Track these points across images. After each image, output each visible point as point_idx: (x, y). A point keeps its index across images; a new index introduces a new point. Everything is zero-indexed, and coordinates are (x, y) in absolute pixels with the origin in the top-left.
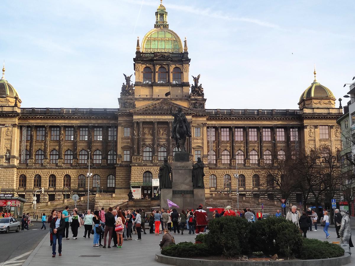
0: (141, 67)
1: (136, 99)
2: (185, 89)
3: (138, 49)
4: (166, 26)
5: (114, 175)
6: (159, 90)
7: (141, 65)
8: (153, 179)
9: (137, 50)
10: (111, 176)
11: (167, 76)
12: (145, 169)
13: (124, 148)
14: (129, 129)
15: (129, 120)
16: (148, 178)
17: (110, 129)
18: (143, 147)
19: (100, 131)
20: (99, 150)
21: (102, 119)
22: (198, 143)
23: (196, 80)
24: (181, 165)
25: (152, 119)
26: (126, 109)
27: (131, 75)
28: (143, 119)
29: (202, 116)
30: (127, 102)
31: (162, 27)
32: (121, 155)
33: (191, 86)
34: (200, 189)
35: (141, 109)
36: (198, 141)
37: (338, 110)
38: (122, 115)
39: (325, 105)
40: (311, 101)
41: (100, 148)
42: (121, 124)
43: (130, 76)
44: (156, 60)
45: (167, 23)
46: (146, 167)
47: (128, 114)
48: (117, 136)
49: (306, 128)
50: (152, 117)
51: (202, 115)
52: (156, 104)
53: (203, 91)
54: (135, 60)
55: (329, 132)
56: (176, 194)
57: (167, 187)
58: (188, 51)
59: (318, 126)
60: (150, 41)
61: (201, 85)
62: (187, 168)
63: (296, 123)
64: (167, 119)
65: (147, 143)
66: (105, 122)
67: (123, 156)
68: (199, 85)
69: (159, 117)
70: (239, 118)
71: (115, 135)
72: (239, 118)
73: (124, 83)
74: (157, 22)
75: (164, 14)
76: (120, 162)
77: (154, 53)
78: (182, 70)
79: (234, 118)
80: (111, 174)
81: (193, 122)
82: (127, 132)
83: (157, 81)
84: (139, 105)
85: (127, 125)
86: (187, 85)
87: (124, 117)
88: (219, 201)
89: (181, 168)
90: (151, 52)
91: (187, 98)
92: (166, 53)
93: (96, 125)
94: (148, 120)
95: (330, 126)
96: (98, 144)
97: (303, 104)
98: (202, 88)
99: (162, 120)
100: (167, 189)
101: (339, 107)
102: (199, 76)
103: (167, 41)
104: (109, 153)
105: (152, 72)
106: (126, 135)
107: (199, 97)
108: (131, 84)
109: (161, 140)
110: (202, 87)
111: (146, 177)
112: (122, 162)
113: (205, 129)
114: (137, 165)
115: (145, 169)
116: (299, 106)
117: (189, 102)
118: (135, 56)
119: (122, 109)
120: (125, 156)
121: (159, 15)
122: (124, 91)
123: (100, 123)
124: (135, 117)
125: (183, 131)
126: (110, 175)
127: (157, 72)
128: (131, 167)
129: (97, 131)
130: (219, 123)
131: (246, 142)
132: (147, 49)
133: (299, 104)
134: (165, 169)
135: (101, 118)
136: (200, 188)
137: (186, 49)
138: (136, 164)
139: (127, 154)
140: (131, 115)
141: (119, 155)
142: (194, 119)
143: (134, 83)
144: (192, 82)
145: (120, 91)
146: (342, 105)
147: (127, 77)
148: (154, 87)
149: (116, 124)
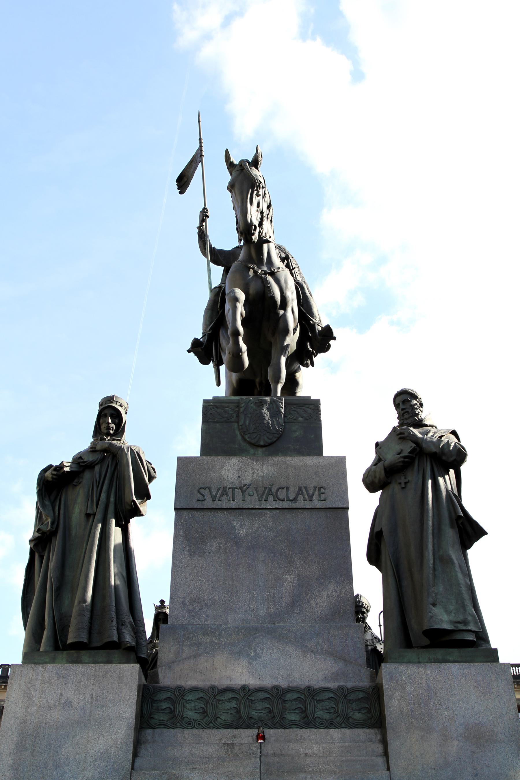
24: (248, 479)
34: (455, 668)
56: (190, 724)
62: (301, 503)
89: (252, 502)
100: (78, 661)
136: (455, 652)
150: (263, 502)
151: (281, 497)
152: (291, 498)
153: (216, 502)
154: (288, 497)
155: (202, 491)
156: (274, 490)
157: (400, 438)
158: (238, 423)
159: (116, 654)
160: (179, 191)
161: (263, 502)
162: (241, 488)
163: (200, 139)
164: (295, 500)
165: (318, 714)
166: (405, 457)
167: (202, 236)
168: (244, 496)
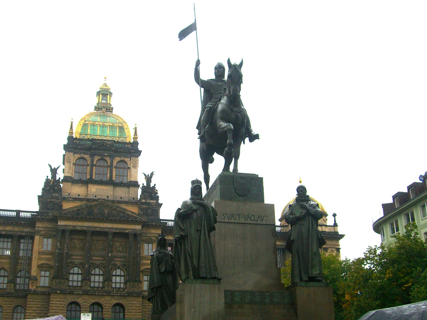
0: (73, 157)
1: (64, 199)
2: (132, 189)
3: (71, 133)
4: (109, 109)
5: (24, 307)
6: (96, 188)
7: (74, 155)
8: (82, 314)
9: (70, 135)
10: (19, 308)
11: (109, 172)
12: (70, 299)
13: (41, 267)
14: (50, 241)
15: (52, 228)
16: (73, 313)
17: (22, 241)
18: (69, 266)
19: (8, 242)
20: (5, 270)
21: (12, 224)
23: (149, 179)
25: (85, 227)
26: (48, 212)
27: (59, 167)
28: (72, 226)
29: (156, 227)
30: (51, 202)
31: (104, 110)
32: (36, 277)
33: (141, 186)
35: (70, 212)
37: (333, 228)
38: (42, 220)
41: (6, 267)
42: (38, 232)
43: (58, 168)
44: (95, 149)
45: (112, 106)
46: (71, 296)
47: (50, 219)
48: (32, 250)
50: (86, 224)
51: (156, 225)
52: (91, 206)
53: (157, 193)
54: (66, 147)
57: (204, 275)
58: (138, 141)
60: (87, 125)
61: (155, 185)
62: (259, 222)
64: (107, 228)
65: (77, 262)
66: (16, 229)
67: (39, 279)
68: (152, 185)
69: (96, 225)
71: (29, 248)
73: (47, 177)
74: (98, 104)
75: (107, 95)
76: (34, 288)
77: (93, 140)
78: (129, 165)
80: (19, 305)
81: (143, 235)
82: (47, 244)
83: (94, 178)
84: (66, 206)
85: (48, 235)
86: (136, 184)
87: (46, 223)
89: (242, 220)
90: (88, 139)
91: (134, 202)
92: (108, 140)
93: (4, 233)
94: (78, 228)
96: (4, 261)
98: (157, 190)
99: (99, 229)
101: (334, 224)
102: (152, 174)
103: (110, 127)
104: (19, 275)
105: (88, 165)
106: (45, 249)
107: (152, 202)
108: (57, 179)
109: (94, 258)
110: (156, 189)
111: (71, 311)
112: (37, 287)
114: (59, 292)
115: (70, 299)
117: (139, 207)
118: (66, 142)
119: (42, 211)
120: (42, 278)
121: (101, 95)
122: (47, 187)
123: (9, 231)
124: (61, 223)
125: (239, 115)
126: (17, 306)
127: (95, 165)
128: (49, 294)
129: (4, 241)
132: (83, 134)
134: (195, 215)
135: (12, 223)
137: (135, 138)
138: (58, 290)
139: (45, 276)
140: (55, 220)
141: (34, 276)
142: (144, 230)
143: (62, 178)
144: (142, 181)
145: (42, 186)
147: (53, 168)
148: (89, 185)
149: (32, 232)
150: (246, 221)
151: (253, 219)
152: (256, 219)
153: (229, 220)
154: (254, 219)
155: (224, 215)
156: (250, 216)
157: (301, 207)
158: (233, 185)
159: (216, 281)
160: (179, 39)
161: (246, 221)
162: (238, 215)
163: (195, 20)
164: (257, 221)
165: (275, 300)
166: (303, 215)
168: (239, 218)
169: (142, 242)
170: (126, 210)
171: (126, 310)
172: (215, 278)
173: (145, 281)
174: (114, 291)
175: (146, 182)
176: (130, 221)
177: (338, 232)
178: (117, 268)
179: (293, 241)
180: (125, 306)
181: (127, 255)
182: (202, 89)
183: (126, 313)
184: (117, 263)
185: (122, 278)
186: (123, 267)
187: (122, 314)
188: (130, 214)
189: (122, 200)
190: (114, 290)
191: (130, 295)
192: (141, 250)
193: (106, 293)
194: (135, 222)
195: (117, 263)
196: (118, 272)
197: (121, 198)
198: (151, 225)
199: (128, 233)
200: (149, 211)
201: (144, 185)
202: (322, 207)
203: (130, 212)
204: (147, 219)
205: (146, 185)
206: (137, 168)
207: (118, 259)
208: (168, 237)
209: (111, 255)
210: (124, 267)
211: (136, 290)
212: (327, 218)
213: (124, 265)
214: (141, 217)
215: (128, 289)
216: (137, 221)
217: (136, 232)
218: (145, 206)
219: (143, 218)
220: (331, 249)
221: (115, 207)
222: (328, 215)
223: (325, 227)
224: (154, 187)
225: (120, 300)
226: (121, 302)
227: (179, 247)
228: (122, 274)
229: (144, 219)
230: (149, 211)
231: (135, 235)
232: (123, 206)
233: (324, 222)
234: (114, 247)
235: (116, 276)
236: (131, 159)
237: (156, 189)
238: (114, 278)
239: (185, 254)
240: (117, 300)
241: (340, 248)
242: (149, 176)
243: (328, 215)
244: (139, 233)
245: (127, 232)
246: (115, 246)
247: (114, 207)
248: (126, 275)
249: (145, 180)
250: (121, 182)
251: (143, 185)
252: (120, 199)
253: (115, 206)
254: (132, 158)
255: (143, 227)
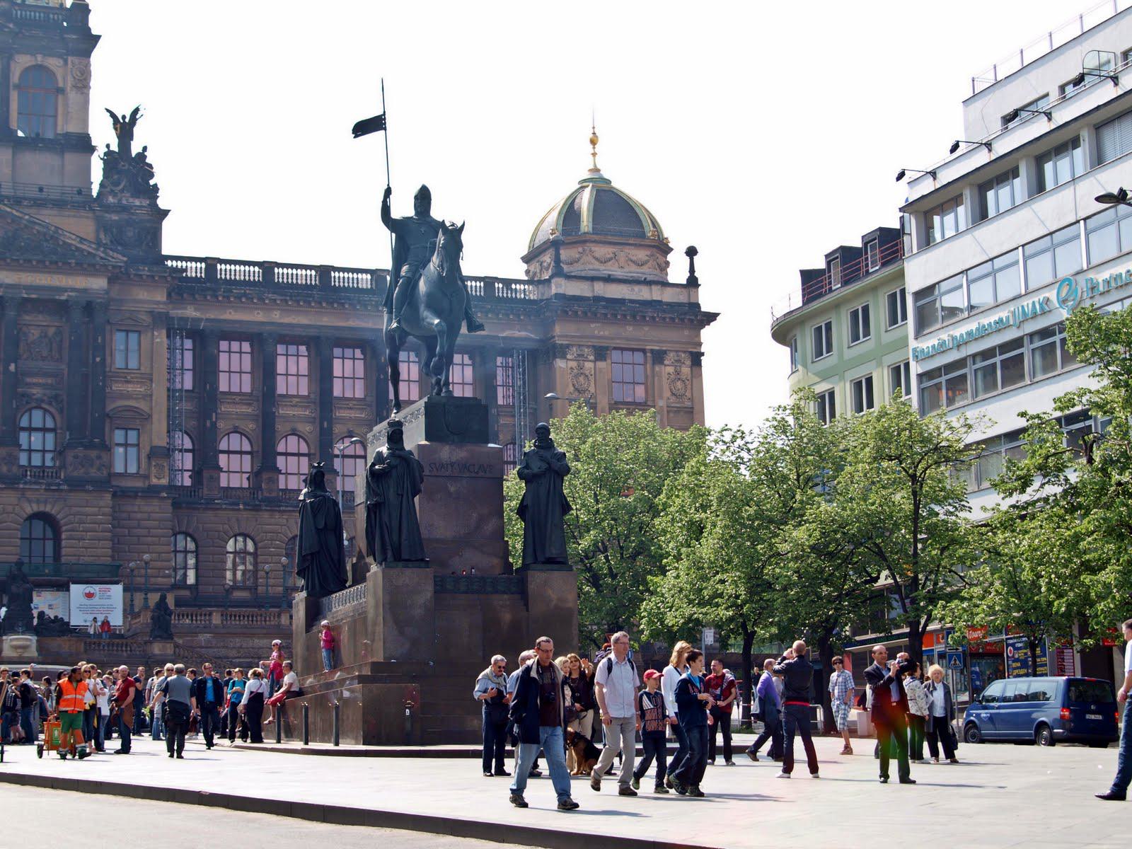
2: (71, 159)
22: (128, 396)
23: (125, 128)
24: (454, 459)
33: (101, 151)
36: (130, 388)
39: (634, 268)
40: (580, 249)
49: (564, 357)
53: (152, 175)
55: (646, 377)
57: (407, 557)
59: (607, 348)
61: (145, 149)
62: (481, 474)
63: (523, 334)
68: (135, 149)
70: (298, 298)
72: (298, 298)
79: (275, 300)
86: (84, 145)
88: (237, 641)
91: (80, 200)
95: (652, 351)
97: (547, 258)
98: (150, 166)
107: (137, 203)
110: (148, 161)
113: (161, 337)
116: (525, 267)
130: (212, 317)
131: (323, 399)
133: (527, 259)
134: (394, 472)
136: (555, 566)
146: (696, 274)
159: (423, 564)
163: (384, 112)
164: (477, 473)
167: (386, 210)
169: (108, 328)
170: (60, 232)
171: (66, 531)
172: (422, 560)
173: (118, 445)
174: (26, 475)
175: (116, 141)
176: (73, 265)
177: (698, 306)
178: (36, 408)
179: (526, 506)
180: (62, 522)
181: (64, 367)
182: (394, 235)
183: (64, 543)
184: (34, 391)
185: (50, 437)
186: (50, 404)
187: (49, 545)
188: (73, 242)
189: (44, 195)
190: (29, 473)
191: (77, 485)
192: (108, 352)
193: (5, 484)
194: (86, 265)
195: (34, 391)
196: (37, 418)
197: (41, 190)
198: (136, 275)
199: (67, 300)
200: (130, 234)
201: (111, 149)
202: (654, 226)
203: (74, 237)
204: (125, 259)
205: (116, 150)
206: (85, 91)
207: (35, 380)
208: (186, 309)
209: (16, 367)
210: (54, 404)
211: (93, 472)
212: (670, 257)
213: (56, 397)
214: (107, 254)
215: (70, 469)
216: (94, 265)
217: (89, 299)
218: (117, 218)
219: (113, 258)
220: (674, 353)
221: (26, 220)
222: (672, 249)
223: (659, 287)
224: (142, 156)
225: (46, 502)
226: (48, 509)
227: (373, 516)
228: (50, 424)
229: (119, 259)
230: (130, 234)
231: (89, 307)
232: (49, 217)
233: (658, 272)
234: (22, 345)
235: (30, 429)
236: (66, 62)
237: (148, 161)
238: (23, 437)
239: (381, 528)
240: (38, 502)
241: (703, 354)
242: (127, 120)
243: (672, 249)
244: (99, 301)
245: (64, 298)
246: (26, 340)
247: (25, 222)
248: (61, 429)
249: (113, 132)
250: (38, 135)
251: (106, 150)
252: (34, 193)
253: (27, 217)
254: (69, 62)
255: (111, 281)
